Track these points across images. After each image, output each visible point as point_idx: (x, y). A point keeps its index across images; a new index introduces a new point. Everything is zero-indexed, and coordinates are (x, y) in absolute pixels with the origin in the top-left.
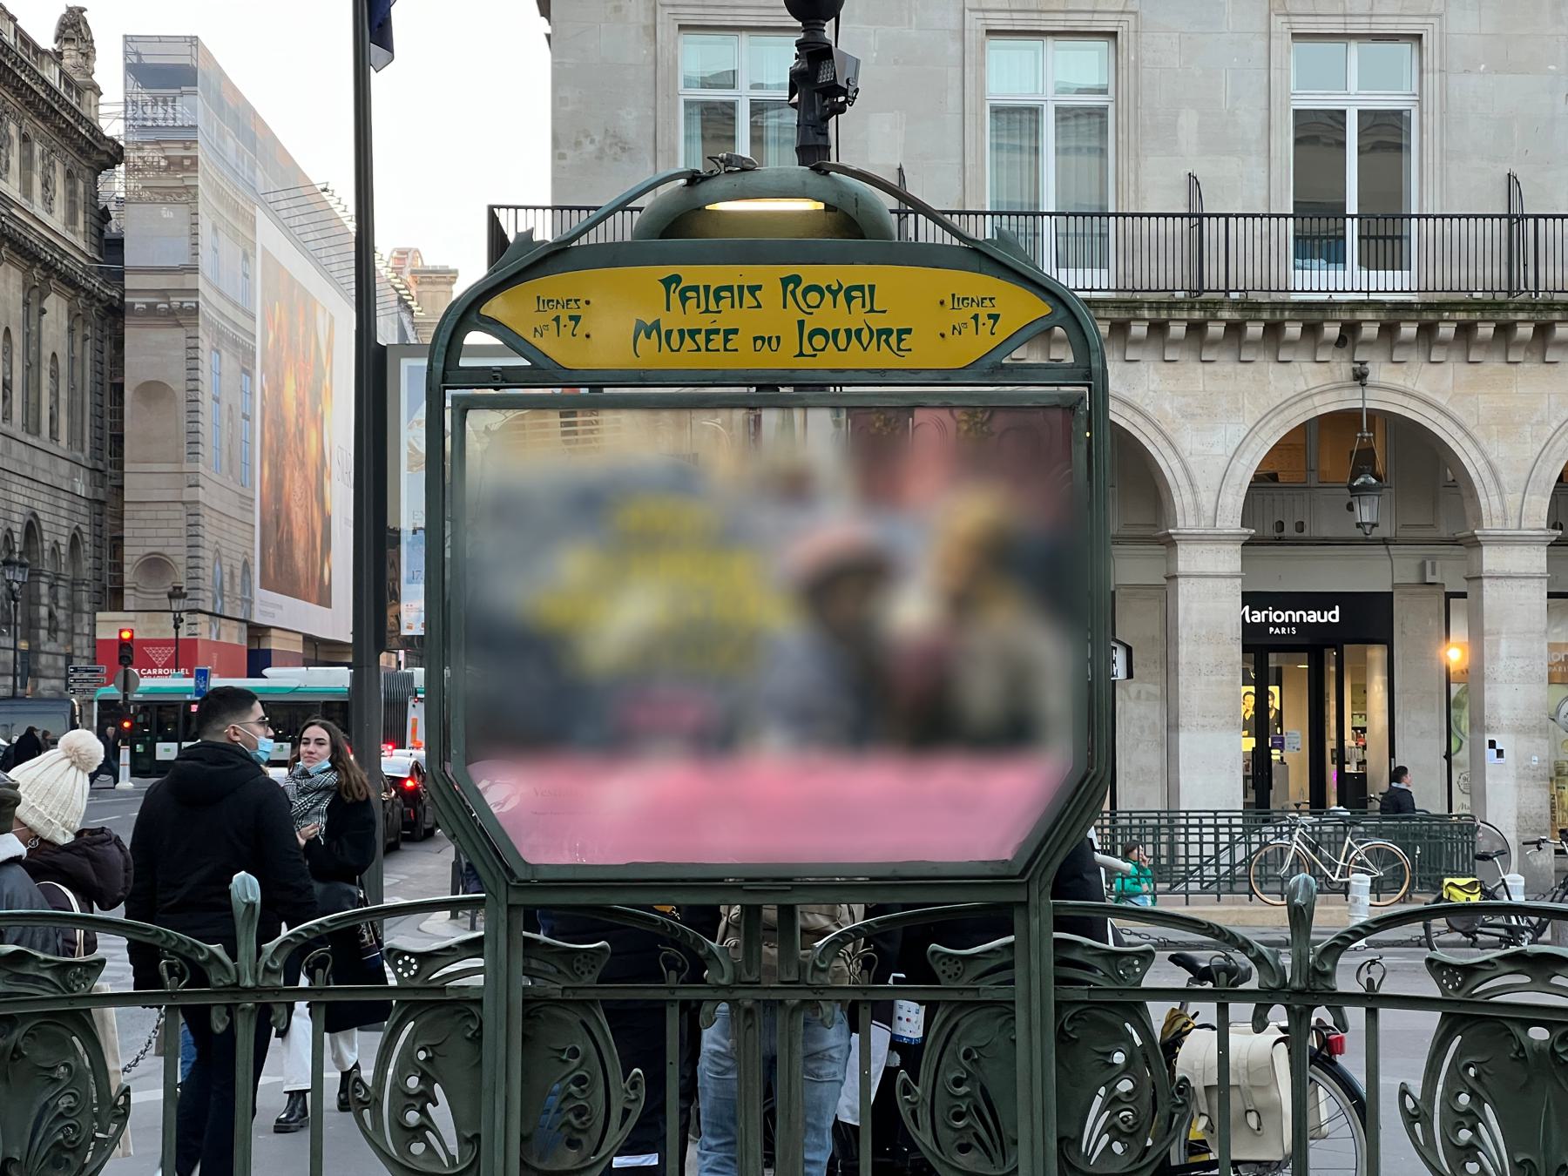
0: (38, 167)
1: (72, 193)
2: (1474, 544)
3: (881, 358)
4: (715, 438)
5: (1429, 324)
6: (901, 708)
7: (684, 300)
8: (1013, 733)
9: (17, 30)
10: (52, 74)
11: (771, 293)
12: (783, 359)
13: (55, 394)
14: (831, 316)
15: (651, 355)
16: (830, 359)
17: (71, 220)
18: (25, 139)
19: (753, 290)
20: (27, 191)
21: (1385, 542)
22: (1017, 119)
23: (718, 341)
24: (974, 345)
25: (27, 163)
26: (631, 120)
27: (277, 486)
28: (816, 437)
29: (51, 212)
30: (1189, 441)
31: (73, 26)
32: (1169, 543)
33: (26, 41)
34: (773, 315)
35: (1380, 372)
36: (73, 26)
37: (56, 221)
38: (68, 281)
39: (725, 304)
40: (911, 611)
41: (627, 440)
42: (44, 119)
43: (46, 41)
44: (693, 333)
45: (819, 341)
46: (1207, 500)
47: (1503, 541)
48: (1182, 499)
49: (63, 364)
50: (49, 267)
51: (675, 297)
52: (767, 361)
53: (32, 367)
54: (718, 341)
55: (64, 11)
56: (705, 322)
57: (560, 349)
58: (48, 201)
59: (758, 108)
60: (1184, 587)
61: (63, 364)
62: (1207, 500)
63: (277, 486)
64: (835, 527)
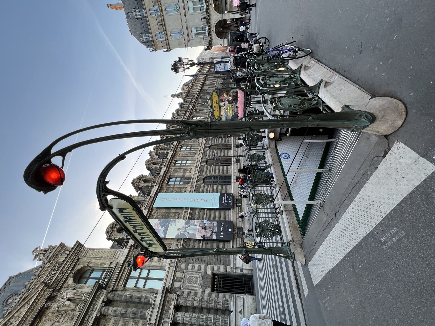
3: (217, 100)
4: (223, 109)
5: (209, 23)
6: (235, 99)
8: (237, 92)
12: (218, 105)
14: (215, 103)
15: (218, 111)
22: (194, 9)
24: (216, 95)
26: (198, 41)
27: (221, 51)
28: (222, 103)
34: (216, 105)
40: (230, 98)
41: (223, 112)
57: (218, 115)
59: (197, 31)
63: (221, 51)
64: (226, 102)
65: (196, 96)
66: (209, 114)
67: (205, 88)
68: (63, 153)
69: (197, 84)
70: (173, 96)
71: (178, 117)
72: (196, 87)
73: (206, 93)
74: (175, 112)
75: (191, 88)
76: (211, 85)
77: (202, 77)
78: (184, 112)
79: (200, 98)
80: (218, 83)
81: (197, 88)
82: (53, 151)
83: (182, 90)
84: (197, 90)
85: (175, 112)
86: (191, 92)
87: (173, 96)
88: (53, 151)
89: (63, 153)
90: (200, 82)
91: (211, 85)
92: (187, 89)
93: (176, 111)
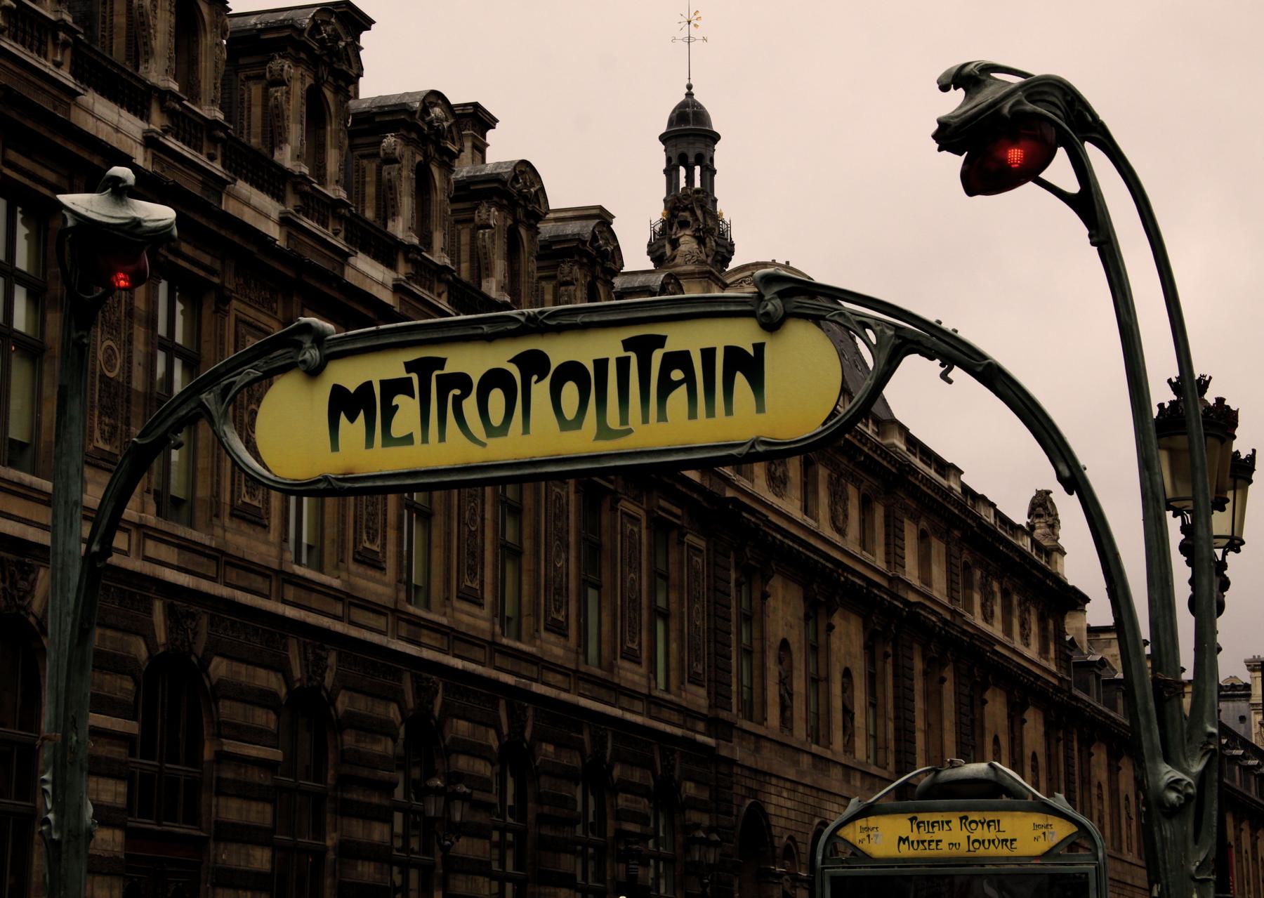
0: (1017, 612)
1: (1043, 629)
3: (1004, 851)
7: (919, 827)
9: (998, 514)
10: (1025, 543)
11: (955, 823)
14: (980, 833)
16: (981, 852)
17: (1044, 651)
18: (1006, 594)
19: (948, 822)
20: (1008, 631)
23: (933, 845)
24: (1041, 847)
29: (1027, 645)
37: (1032, 652)
39: (936, 829)
43: (1020, 517)
44: (923, 842)
45: (976, 845)
49: (1042, 760)
51: (915, 827)
54: (933, 845)
55: (1034, 494)
56: (927, 837)
58: (1025, 638)
61: (1042, 760)
66: (454, 638)
68: (1087, 204)
69: (838, 498)
70: (689, 136)
71: (439, 196)
74: (501, 149)
76: (817, 681)
77: (911, 573)
79: (660, 527)
80: (834, 780)
82: (1093, 153)
85: (501, 149)
87: (689, 136)
88: (1093, 153)
89: (1087, 204)
90: (851, 542)
91: (817, 681)
93: (525, 170)
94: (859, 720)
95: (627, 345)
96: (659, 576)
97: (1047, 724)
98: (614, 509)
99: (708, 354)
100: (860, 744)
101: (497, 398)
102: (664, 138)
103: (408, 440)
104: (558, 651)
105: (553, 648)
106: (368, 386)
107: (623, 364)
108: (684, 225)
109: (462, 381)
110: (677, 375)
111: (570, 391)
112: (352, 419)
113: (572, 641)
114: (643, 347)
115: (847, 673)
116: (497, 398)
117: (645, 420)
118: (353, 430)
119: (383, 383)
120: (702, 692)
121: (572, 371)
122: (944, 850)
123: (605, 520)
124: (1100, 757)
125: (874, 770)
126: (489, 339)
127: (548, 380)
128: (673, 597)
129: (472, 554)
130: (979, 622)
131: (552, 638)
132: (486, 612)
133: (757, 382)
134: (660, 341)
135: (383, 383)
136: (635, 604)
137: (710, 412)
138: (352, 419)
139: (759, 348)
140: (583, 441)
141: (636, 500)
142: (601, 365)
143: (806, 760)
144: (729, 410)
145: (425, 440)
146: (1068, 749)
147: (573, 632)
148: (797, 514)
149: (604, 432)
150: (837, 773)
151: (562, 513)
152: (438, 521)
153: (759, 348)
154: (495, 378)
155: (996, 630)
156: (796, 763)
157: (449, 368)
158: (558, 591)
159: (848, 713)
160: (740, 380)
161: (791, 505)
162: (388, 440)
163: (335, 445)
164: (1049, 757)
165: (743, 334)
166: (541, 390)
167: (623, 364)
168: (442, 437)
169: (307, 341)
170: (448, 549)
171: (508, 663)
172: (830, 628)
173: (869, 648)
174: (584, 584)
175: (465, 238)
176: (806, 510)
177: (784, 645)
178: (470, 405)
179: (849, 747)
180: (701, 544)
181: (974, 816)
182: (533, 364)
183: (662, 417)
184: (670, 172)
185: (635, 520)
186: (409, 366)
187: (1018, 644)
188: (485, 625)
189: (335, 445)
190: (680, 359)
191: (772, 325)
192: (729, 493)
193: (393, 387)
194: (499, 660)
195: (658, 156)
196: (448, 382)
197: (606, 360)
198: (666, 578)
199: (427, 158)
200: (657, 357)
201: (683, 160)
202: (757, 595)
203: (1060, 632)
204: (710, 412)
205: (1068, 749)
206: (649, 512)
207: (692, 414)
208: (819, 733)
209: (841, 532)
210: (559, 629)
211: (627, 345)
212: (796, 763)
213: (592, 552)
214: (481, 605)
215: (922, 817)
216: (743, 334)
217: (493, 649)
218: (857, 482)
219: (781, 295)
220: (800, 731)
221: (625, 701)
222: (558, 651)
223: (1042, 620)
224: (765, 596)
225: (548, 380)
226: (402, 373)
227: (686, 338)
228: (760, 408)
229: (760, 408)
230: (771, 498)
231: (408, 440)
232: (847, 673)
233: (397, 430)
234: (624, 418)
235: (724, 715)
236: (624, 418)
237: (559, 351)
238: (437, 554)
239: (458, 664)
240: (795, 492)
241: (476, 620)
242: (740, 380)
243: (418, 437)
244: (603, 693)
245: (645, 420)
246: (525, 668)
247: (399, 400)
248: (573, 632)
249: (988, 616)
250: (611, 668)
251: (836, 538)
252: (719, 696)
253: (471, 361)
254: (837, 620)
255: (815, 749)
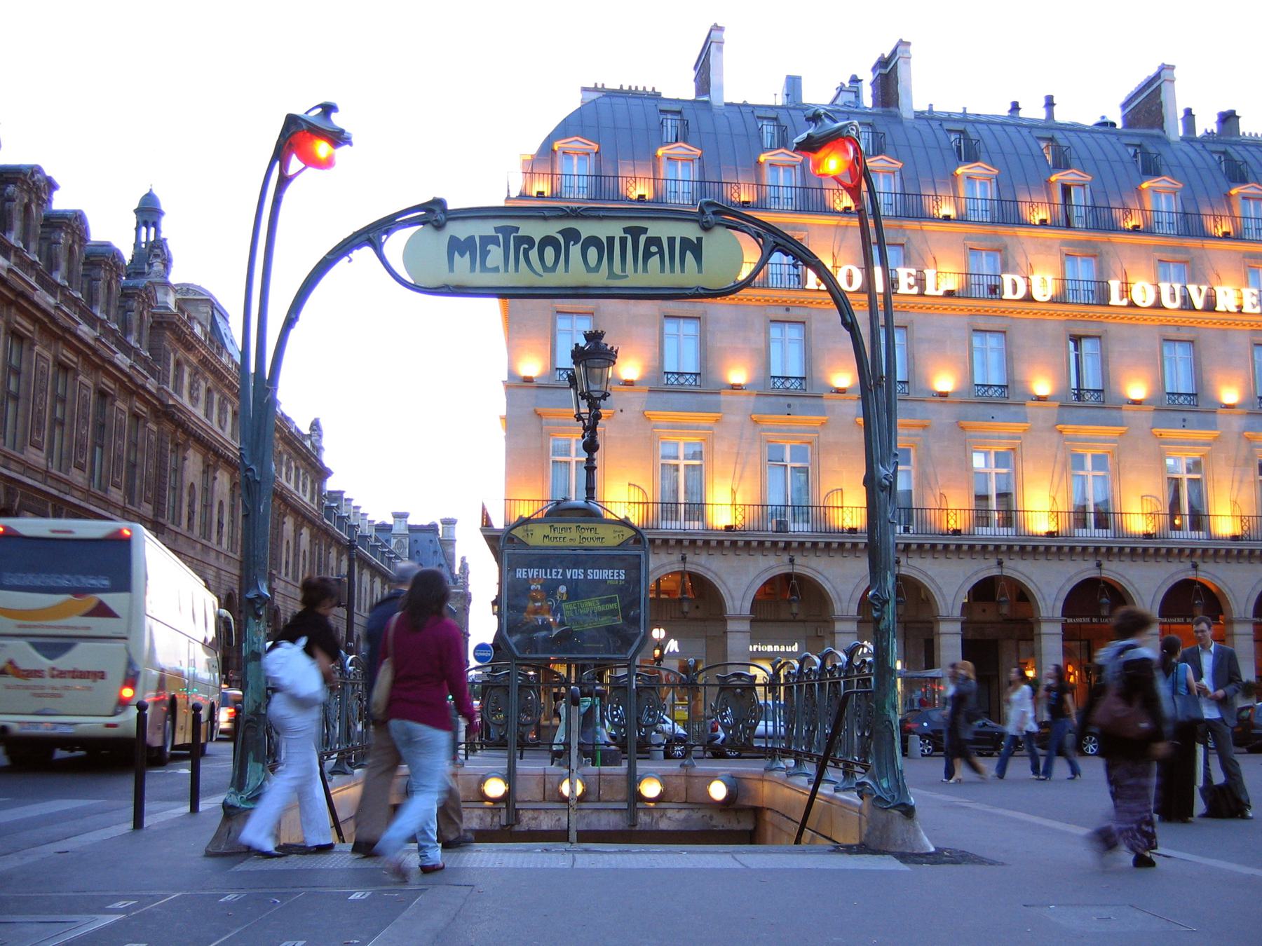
1: (313, 488)
2: (833, 621)
3: (598, 544)
10: (308, 443)
12: (577, 543)
13: (304, 566)
14: (587, 534)
16: (586, 544)
17: (312, 499)
18: (297, 468)
20: (297, 488)
21: (804, 621)
24: (617, 541)
25: (297, 477)
30: (730, 584)
31: (315, 426)
32: (724, 621)
33: (298, 431)
35: (799, 560)
36: (315, 426)
37: (307, 499)
38: (311, 523)
42: (304, 459)
43: (306, 431)
46: (738, 604)
47: (842, 620)
48: (729, 604)
49: (307, 554)
50: (304, 517)
52: (572, 544)
53: (296, 555)
58: (304, 491)
60: (729, 635)
61: (307, 554)
62: (738, 604)
65: (151, 385)
66: (28, 468)
67: (193, 463)
69: (222, 410)
70: (148, 212)
72: (202, 394)
73: (161, 466)
75: (204, 362)
76: (207, 506)
78: (58, 277)
79: (136, 416)
81: (194, 399)
83: (186, 288)
84: (185, 400)
86: (181, 353)
87: (148, 212)
91: (207, 506)
92: (198, 330)
94: (225, 529)
95: (626, 230)
96: (134, 445)
97: (313, 537)
98: (112, 404)
99: (671, 240)
100: (225, 540)
101: (549, 252)
102: (136, 211)
103: (496, 269)
104: (80, 479)
105: (78, 477)
106: (472, 238)
107: (623, 241)
108: (157, 256)
109: (529, 241)
110: (654, 249)
111: (592, 253)
112: (462, 255)
113: (87, 476)
114: (636, 232)
115: (221, 503)
116: (549, 252)
117: (636, 271)
118: (462, 262)
119: (481, 237)
120: (150, 507)
121: (593, 241)
122: (568, 543)
123: (108, 409)
124: (334, 553)
125: (230, 554)
126: (545, 218)
127: (579, 245)
128: (139, 456)
129: (39, 423)
130: (283, 480)
131: (78, 471)
132: (44, 455)
133: (698, 258)
134: (645, 230)
135: (481, 237)
136: (120, 458)
137: (672, 270)
138: (462, 255)
139: (700, 240)
140: (600, 279)
141: (124, 401)
142: (611, 240)
143: (199, 546)
144: (683, 271)
145: (506, 270)
146: (320, 549)
147: (87, 470)
148: (203, 417)
149: (611, 275)
150: (213, 554)
151: (86, 406)
152: (21, 401)
153: (700, 240)
154: (548, 241)
155: (291, 486)
156: (194, 548)
157: (520, 233)
158: (81, 447)
159: (220, 524)
160: (688, 253)
161: (199, 412)
162: (484, 268)
163: (451, 269)
164: (312, 553)
165: (690, 231)
166: (575, 250)
167: (623, 241)
168: (517, 269)
169: (438, 210)
170: (26, 418)
171: (55, 484)
172: (215, 478)
173: (232, 490)
174: (95, 444)
175: (44, 248)
176: (207, 415)
177: (192, 485)
178: (534, 254)
179: (220, 542)
180: (155, 428)
181: (582, 525)
182: (572, 235)
183: (645, 269)
184: (138, 229)
185: (123, 412)
186: (497, 230)
187: (301, 494)
188: (43, 461)
189: (451, 269)
190: (656, 241)
191: (706, 228)
192: (171, 402)
193: (486, 240)
194: (49, 481)
195: (132, 220)
196: (521, 240)
197: (613, 238)
198: (136, 445)
199: (30, 201)
200: (642, 239)
201: (146, 224)
202: (180, 458)
203: (320, 490)
204: (672, 270)
205: (320, 549)
206: (130, 409)
207: (662, 270)
208: (206, 534)
209: (222, 428)
210: (81, 467)
211: (626, 230)
212: (194, 548)
213: (100, 427)
214: (41, 450)
215: (556, 525)
216: (690, 231)
217: (47, 474)
218: (232, 403)
219: (714, 213)
220: (197, 531)
221: (112, 509)
222: (80, 479)
223: (312, 482)
224: (184, 459)
225: (579, 245)
226: (493, 233)
227: (659, 229)
228: (700, 271)
229: (700, 271)
230: (190, 407)
231: (496, 269)
232: (221, 503)
233: (490, 262)
234: (623, 270)
235: (161, 520)
236: (623, 270)
237: (587, 229)
238: (20, 420)
239: (30, 482)
240: (202, 404)
241: (36, 457)
242: (688, 253)
243: (502, 269)
244: (102, 504)
245: (636, 271)
246: (63, 487)
247: (490, 247)
248: (87, 470)
249: (288, 480)
250: (106, 491)
251: (220, 431)
252: (159, 510)
253: (536, 230)
254: (218, 474)
255: (204, 541)
